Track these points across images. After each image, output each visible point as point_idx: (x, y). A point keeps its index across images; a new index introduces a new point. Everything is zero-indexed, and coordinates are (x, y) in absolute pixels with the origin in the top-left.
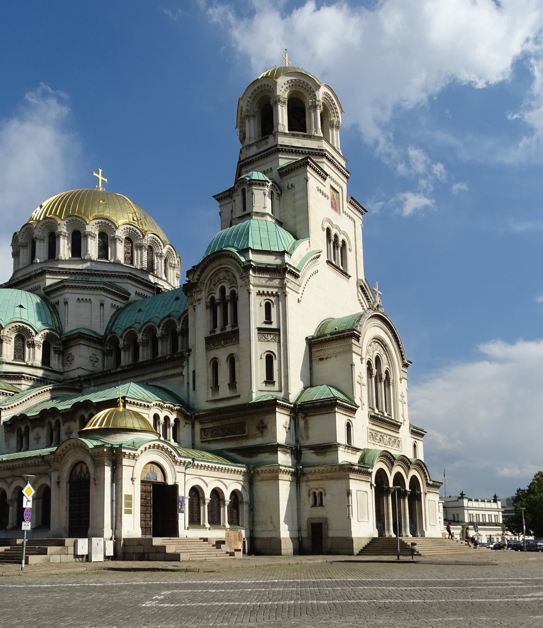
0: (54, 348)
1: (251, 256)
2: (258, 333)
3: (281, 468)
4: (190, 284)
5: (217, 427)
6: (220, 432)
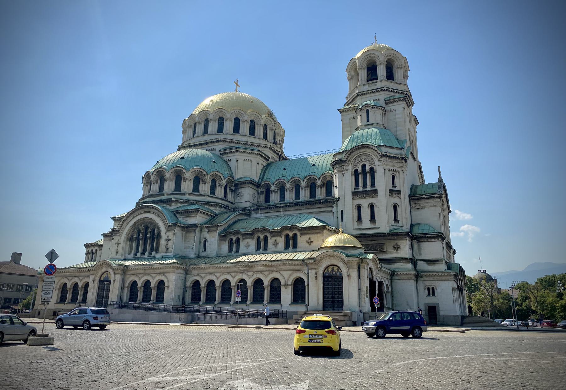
0: (229, 188)
2: (389, 193)
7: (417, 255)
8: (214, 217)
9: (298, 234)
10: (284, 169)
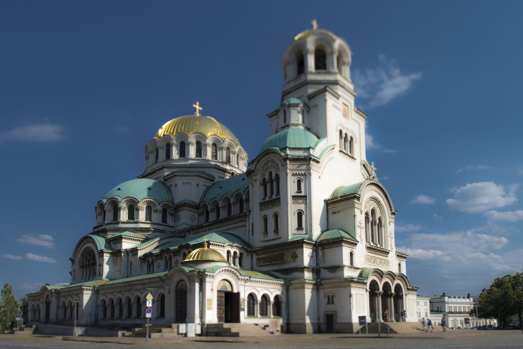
0: (169, 212)
1: (288, 152)
2: (293, 199)
3: (306, 281)
4: (250, 171)
5: (267, 257)
6: (269, 260)
8: (145, 241)
10: (221, 187)
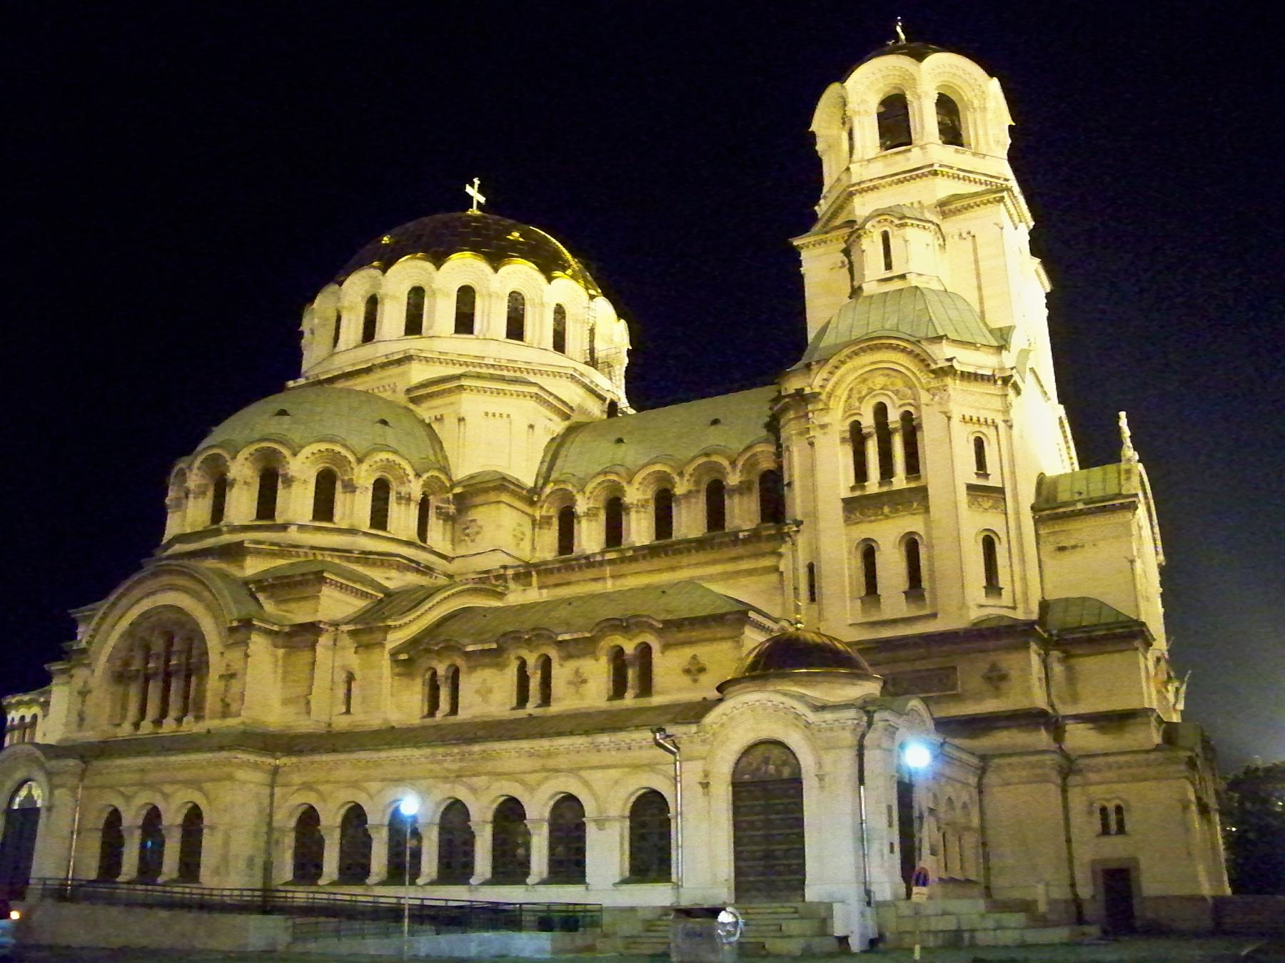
0: (438, 508)
7: (1064, 703)
9: (656, 645)
